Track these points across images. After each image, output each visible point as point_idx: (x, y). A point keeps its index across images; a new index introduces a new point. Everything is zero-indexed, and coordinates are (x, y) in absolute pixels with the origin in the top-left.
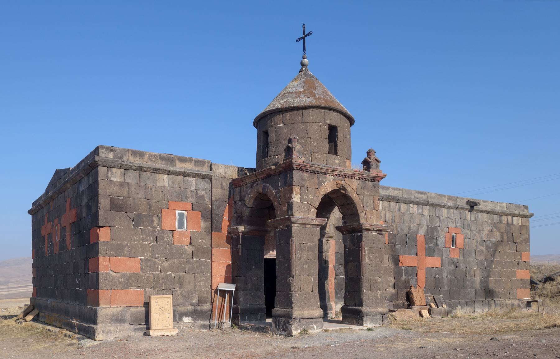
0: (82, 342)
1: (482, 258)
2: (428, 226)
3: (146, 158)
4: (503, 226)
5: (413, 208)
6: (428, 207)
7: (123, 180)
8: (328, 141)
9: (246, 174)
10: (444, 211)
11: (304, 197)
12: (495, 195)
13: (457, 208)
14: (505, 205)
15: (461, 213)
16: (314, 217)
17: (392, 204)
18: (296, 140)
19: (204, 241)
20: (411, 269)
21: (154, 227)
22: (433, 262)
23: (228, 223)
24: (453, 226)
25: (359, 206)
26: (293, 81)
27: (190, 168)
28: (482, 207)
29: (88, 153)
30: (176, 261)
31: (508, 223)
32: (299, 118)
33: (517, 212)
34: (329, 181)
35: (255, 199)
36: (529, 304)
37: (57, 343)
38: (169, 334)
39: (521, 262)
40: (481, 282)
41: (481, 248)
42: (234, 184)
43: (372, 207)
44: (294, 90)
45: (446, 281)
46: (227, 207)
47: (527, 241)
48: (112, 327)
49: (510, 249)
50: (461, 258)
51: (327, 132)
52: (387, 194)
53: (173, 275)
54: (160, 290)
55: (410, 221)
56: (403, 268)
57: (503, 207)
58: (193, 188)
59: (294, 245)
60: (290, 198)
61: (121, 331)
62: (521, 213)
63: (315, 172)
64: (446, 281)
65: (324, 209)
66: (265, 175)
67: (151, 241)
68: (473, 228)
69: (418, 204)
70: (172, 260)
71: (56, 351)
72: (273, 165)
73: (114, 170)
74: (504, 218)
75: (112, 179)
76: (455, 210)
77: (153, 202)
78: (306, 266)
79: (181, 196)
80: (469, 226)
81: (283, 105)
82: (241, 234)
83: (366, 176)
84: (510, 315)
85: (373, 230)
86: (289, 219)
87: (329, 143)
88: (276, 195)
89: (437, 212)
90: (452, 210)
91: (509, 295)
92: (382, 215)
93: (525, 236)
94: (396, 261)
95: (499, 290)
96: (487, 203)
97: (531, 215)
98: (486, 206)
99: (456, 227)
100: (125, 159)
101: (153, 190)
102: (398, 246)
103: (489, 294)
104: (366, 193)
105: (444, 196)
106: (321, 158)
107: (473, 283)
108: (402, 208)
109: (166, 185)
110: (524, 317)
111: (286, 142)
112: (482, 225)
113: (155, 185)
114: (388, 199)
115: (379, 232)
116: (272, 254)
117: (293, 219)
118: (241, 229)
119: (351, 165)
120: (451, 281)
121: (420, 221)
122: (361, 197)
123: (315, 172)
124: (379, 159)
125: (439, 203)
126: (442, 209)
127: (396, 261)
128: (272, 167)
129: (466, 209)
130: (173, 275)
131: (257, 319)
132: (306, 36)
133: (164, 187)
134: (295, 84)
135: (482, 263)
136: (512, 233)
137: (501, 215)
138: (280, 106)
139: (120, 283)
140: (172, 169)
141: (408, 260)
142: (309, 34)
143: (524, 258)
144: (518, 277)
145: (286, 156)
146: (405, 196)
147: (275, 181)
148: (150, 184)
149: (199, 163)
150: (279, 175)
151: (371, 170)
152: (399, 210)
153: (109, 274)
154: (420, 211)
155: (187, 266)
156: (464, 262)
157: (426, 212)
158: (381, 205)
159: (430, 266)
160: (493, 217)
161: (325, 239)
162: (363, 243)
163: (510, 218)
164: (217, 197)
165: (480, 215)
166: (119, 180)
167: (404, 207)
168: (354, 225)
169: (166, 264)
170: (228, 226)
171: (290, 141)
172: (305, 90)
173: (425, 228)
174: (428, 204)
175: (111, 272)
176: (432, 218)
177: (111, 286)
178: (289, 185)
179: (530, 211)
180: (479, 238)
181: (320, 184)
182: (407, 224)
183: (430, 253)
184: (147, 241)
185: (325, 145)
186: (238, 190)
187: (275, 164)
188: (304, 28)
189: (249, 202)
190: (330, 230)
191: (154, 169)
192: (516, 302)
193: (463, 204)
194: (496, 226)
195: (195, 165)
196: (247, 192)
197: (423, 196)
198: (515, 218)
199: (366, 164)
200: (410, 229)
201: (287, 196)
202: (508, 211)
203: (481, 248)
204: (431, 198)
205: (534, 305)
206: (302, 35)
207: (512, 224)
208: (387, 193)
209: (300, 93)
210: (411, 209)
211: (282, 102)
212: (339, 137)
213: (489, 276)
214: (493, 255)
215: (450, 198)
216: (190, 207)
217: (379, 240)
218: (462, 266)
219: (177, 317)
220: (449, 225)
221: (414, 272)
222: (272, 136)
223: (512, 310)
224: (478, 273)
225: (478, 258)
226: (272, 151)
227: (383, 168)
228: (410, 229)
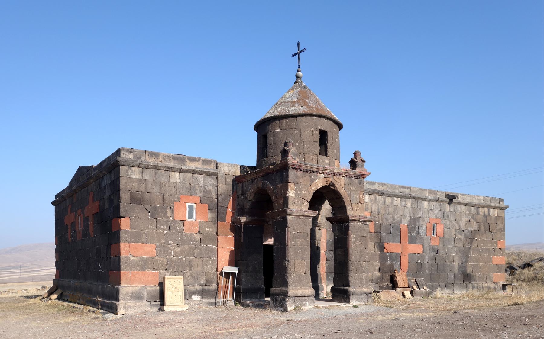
0: (106, 316)
1: (460, 245)
3: (161, 157)
4: (480, 217)
5: (397, 201)
7: (141, 177)
8: (319, 144)
9: (248, 172)
10: (426, 203)
11: (298, 192)
12: (470, 190)
13: (437, 201)
14: (482, 198)
16: (307, 209)
18: (291, 143)
19: (211, 230)
20: (395, 254)
21: (167, 218)
22: (416, 248)
23: (231, 214)
24: (434, 217)
25: (347, 200)
26: (288, 92)
27: (199, 166)
28: (460, 199)
29: (110, 154)
30: (187, 247)
31: (484, 214)
32: (293, 124)
33: (493, 205)
34: (320, 178)
35: (256, 194)
36: (504, 287)
37: (83, 317)
38: (180, 309)
39: (497, 249)
40: (460, 267)
41: (460, 236)
42: (237, 181)
43: (358, 201)
44: (290, 99)
45: (427, 266)
46: (231, 200)
47: (503, 230)
48: (132, 303)
49: (486, 238)
50: (441, 246)
51: (318, 136)
52: (374, 188)
53: (184, 259)
54: (172, 272)
56: (388, 254)
57: (480, 200)
58: (201, 184)
59: (289, 234)
60: (286, 193)
61: (139, 306)
62: (497, 205)
63: (307, 171)
64: (427, 266)
65: (315, 203)
66: (264, 173)
67: (164, 230)
68: (452, 219)
69: (402, 197)
70: (183, 246)
71: (84, 323)
72: (271, 165)
73: (133, 169)
74: (481, 210)
75: (132, 176)
76: (435, 203)
77: (167, 196)
78: (299, 252)
79: (191, 191)
80: (448, 216)
81: (280, 113)
82: (243, 224)
83: (352, 174)
84: (486, 296)
85: (359, 221)
86: (285, 211)
87: (320, 145)
88: (274, 190)
90: (432, 203)
91: (486, 279)
92: (369, 207)
93: (501, 226)
94: (382, 248)
95: (477, 274)
96: (465, 197)
97: (507, 207)
98: (464, 199)
99: (436, 217)
100: (143, 159)
101: (167, 186)
102: (383, 235)
103: (467, 277)
104: (353, 188)
105: (426, 190)
106: (312, 158)
107: (452, 268)
109: (178, 181)
110: (498, 298)
111: (283, 145)
112: (461, 216)
113: (169, 181)
114: (374, 193)
115: (364, 222)
116: (270, 241)
117: (288, 211)
118: (243, 219)
119: (340, 164)
120: (432, 266)
121: (403, 212)
122: (348, 192)
123: (307, 171)
124: (364, 159)
125: (421, 196)
126: (423, 202)
127: (382, 248)
128: (271, 166)
129: (446, 202)
130: (184, 259)
131: (257, 298)
132: (301, 52)
133: (176, 183)
134: (290, 94)
135: (460, 250)
136: (488, 223)
137: (478, 207)
138: (277, 114)
139: (138, 265)
140: (183, 167)
141: (392, 247)
142: (302, 51)
143: (499, 246)
144: (494, 263)
145: (282, 157)
146: (390, 190)
147: (273, 178)
148: (164, 180)
149: (207, 162)
150: (276, 173)
151: (357, 169)
152: (385, 202)
153: (129, 258)
154: (403, 203)
155: (196, 251)
156: (444, 249)
158: (367, 198)
159: (412, 252)
161: (317, 228)
162: (350, 232)
163: (486, 209)
164: (222, 192)
165: (458, 207)
166: (137, 177)
167: (388, 200)
168: (342, 216)
169: (178, 249)
170: (232, 217)
171: (286, 144)
172: (299, 100)
173: (408, 218)
174: (410, 197)
175: (130, 256)
176: (414, 210)
177: (130, 268)
178: (285, 183)
179: (506, 203)
180: (457, 228)
181: (312, 181)
182: (391, 215)
183: (413, 240)
184: (162, 229)
185: (317, 147)
186: (240, 185)
187: (273, 164)
188: (298, 45)
189: (250, 196)
190: (322, 220)
191: (168, 168)
192: (492, 285)
193: (444, 198)
194: (474, 216)
195: (203, 164)
196: (248, 187)
197: (406, 190)
198: (491, 210)
199: (353, 164)
201: (283, 191)
202: (484, 204)
203: (460, 236)
204: (413, 192)
205: (509, 289)
206: (297, 51)
207: (489, 215)
208: (373, 187)
209: (295, 102)
210: (395, 202)
211: (279, 110)
212: (329, 140)
213: (466, 262)
214: (471, 243)
215: (431, 192)
216: (198, 200)
217: (364, 230)
218: (442, 253)
219: (188, 295)
220: (430, 216)
221: (398, 257)
222: (270, 139)
223: (489, 291)
225: (457, 245)
226: (270, 152)
227: (368, 167)
228: (394, 219)
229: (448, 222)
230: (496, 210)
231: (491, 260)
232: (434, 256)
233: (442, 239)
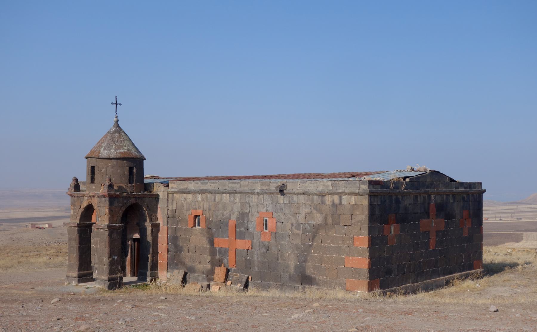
1: (298, 241)
2: (239, 212)
5: (226, 198)
6: (239, 195)
10: (254, 197)
15: (272, 198)
17: (209, 196)
24: (264, 210)
40: (296, 267)
41: (297, 231)
50: (273, 242)
55: (223, 208)
56: (217, 249)
68: (287, 211)
74: (328, 200)
76: (265, 195)
90: (262, 196)
94: (211, 242)
95: (321, 278)
102: (214, 230)
103: (306, 280)
107: (287, 267)
108: (217, 199)
112: (298, 208)
116: (137, 236)
126: (251, 196)
127: (211, 242)
135: (297, 247)
141: (220, 243)
152: (215, 200)
154: (232, 199)
157: (237, 200)
159: (240, 248)
160: (313, 198)
163: (336, 198)
165: (295, 198)
167: (218, 197)
173: (237, 214)
176: (243, 205)
183: (240, 235)
198: (344, 197)
200: (223, 216)
203: (297, 231)
210: (224, 198)
213: (305, 261)
218: (274, 250)
221: (224, 252)
224: (292, 256)
225: (292, 242)
228: (223, 216)
229: (282, 215)
230: (353, 197)
232: (264, 253)
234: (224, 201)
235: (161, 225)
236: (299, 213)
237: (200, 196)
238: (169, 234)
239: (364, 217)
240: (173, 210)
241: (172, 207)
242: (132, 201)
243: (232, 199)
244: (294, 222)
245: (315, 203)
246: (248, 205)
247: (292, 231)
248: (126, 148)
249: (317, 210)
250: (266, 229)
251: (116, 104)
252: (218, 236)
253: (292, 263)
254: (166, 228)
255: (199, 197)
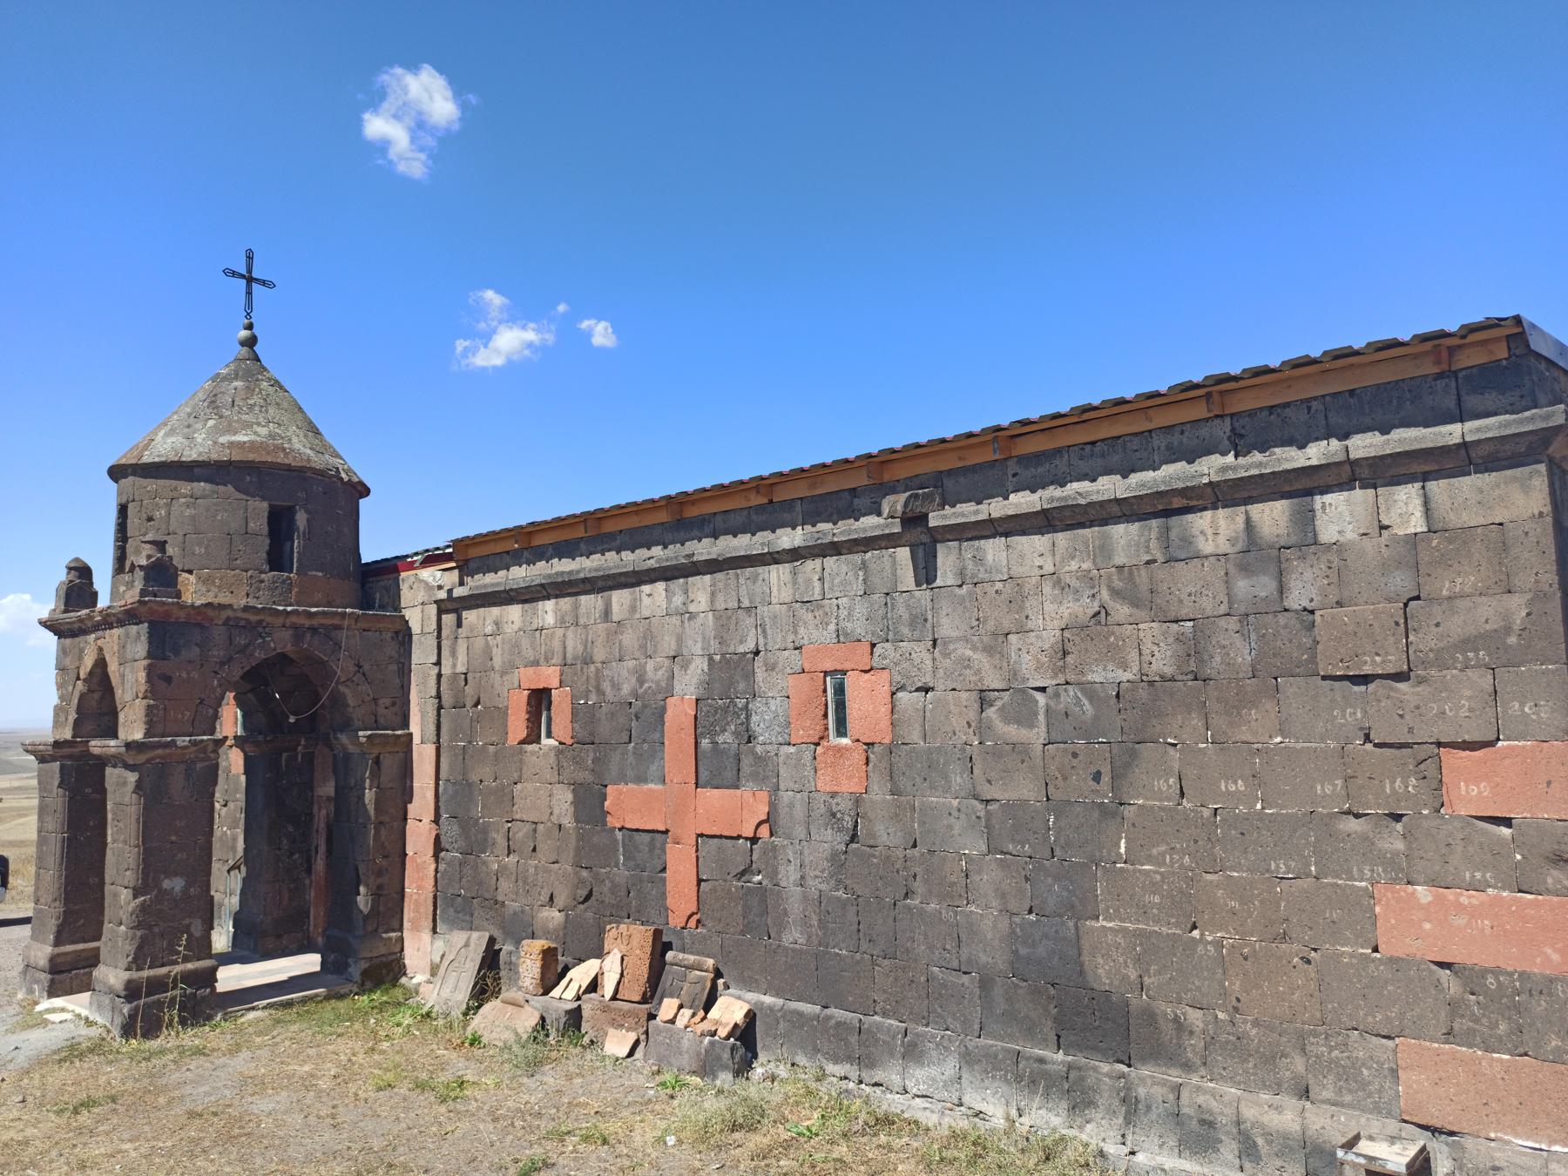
2: (711, 659)
41: (1013, 732)
50: (879, 794)
64: (795, 906)
68: (948, 627)
89: (743, 591)
90: (812, 565)
108: (615, 607)
121: (680, 640)
152: (607, 614)
160: (1106, 537)
173: (699, 666)
176: (725, 621)
182: (631, 664)
183: (718, 768)
200: (641, 681)
203: (1013, 732)
210: (646, 601)
218: (886, 834)
228: (641, 681)
229: (920, 652)
231: (1360, 911)
233: (886, 756)
234: (646, 613)
235: (416, 740)
236: (1022, 631)
237: (549, 605)
238: (443, 775)
239: (1517, 607)
240: (455, 675)
241: (454, 665)
242: (281, 641)
243: (678, 600)
244: (993, 681)
245: (1120, 559)
246: (750, 621)
247: (982, 729)
248: (263, 431)
249: (1135, 603)
250: (841, 730)
251: (250, 280)
252: (622, 779)
253: (988, 918)
254: (430, 750)
255: (548, 611)
